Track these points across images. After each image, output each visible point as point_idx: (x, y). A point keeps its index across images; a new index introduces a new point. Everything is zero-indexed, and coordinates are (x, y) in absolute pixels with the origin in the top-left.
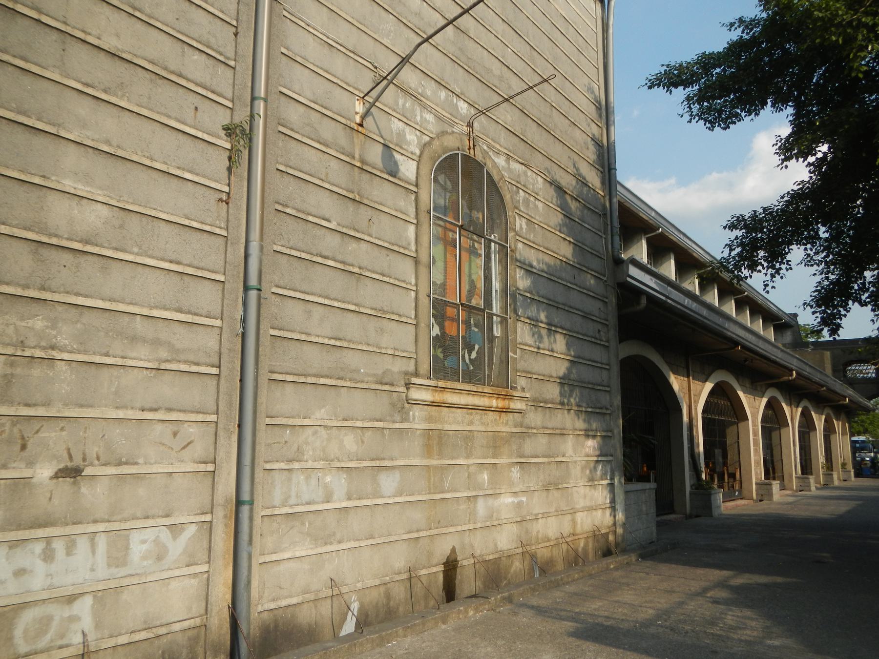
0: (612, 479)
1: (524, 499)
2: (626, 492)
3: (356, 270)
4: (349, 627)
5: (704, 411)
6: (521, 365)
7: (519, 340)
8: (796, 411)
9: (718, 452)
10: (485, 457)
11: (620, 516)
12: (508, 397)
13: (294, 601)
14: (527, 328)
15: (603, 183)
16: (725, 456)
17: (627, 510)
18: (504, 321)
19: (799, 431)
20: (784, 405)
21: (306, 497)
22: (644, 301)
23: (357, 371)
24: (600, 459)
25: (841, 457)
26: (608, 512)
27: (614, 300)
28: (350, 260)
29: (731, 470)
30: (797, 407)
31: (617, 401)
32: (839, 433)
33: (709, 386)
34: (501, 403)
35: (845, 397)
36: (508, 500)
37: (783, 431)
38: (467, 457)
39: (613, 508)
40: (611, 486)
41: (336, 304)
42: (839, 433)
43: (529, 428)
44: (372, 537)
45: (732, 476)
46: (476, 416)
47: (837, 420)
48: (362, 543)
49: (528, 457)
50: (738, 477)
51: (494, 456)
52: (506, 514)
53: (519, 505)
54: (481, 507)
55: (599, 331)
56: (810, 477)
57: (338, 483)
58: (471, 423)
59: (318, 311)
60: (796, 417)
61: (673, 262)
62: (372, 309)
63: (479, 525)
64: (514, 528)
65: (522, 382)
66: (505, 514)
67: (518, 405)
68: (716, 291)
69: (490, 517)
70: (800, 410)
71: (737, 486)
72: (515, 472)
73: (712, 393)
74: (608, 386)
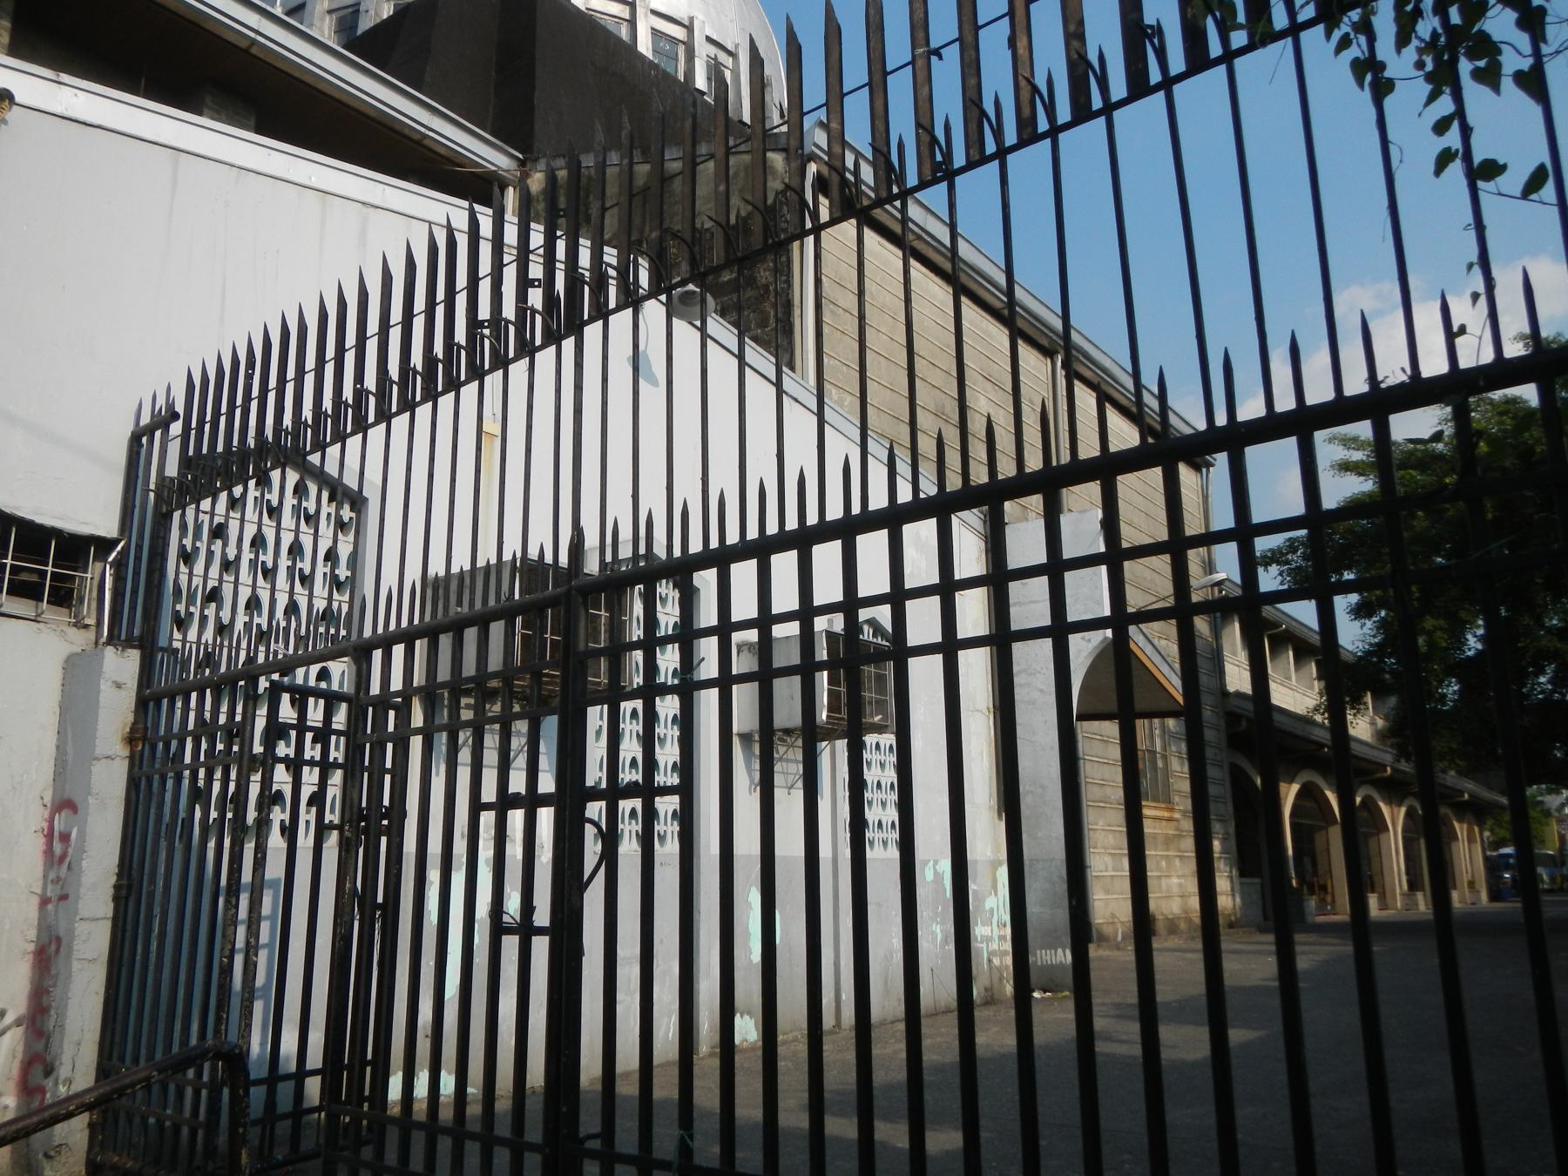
0: (1231, 872)
1: (1183, 881)
2: (1241, 884)
3: (1105, 739)
4: (1119, 938)
5: (1292, 815)
6: (1176, 787)
7: (1173, 769)
8: (1399, 812)
9: (1307, 860)
10: (1163, 851)
11: (1238, 900)
12: (1172, 810)
13: (1101, 921)
14: (1176, 759)
15: (1211, 630)
16: (1314, 864)
17: (1242, 898)
18: (1165, 757)
19: (1404, 838)
20: (1382, 804)
21: (1100, 868)
22: (1244, 724)
23: (1109, 798)
24: (1223, 855)
25: (1467, 873)
26: (1230, 898)
27: (1223, 723)
28: (1103, 734)
29: (1322, 882)
30: (1400, 805)
31: (1230, 808)
32: (1463, 840)
33: (1295, 788)
34: (1166, 814)
35: (1462, 793)
36: (1175, 880)
37: (1383, 837)
38: (1155, 851)
39: (1233, 896)
40: (1231, 878)
41: (1101, 760)
42: (1463, 840)
43: (1182, 831)
44: (1122, 894)
45: (1324, 888)
46: (1157, 824)
47: (1460, 821)
48: (1120, 896)
49: (1183, 852)
50: (1330, 890)
51: (1167, 850)
52: (1175, 890)
53: (1180, 885)
54: (1164, 881)
55: (1216, 754)
56: (1418, 893)
57: (1108, 859)
58: (1155, 828)
59: (1096, 765)
60: (1398, 819)
61: (1237, 625)
62: (1113, 760)
63: (1164, 895)
64: (1178, 900)
65: (1177, 799)
66: (1175, 890)
67: (1177, 816)
68: (1291, 653)
69: (1168, 891)
70: (1403, 810)
71: (1329, 899)
72: (1177, 860)
73: (1299, 795)
74: (1224, 798)
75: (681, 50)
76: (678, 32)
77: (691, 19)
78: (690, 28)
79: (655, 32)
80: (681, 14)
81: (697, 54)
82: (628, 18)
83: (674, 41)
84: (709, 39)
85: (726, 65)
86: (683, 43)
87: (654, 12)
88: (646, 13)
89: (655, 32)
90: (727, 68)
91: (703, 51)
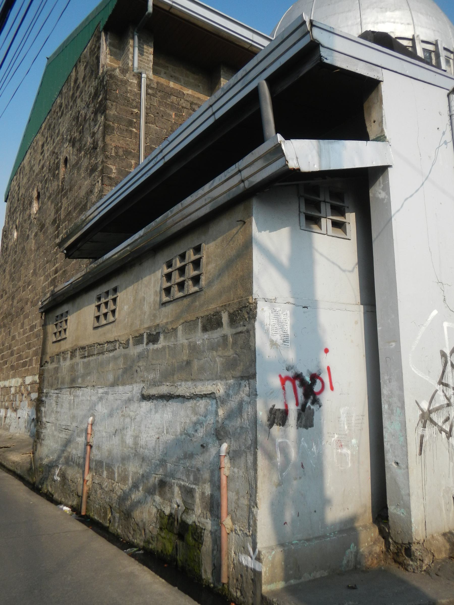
75: (433, 55)
76: (431, 47)
77: (437, 41)
78: (436, 45)
79: (424, 50)
80: (432, 40)
81: (441, 55)
82: (411, 45)
83: (430, 52)
84: (445, 49)
85: (450, 57)
86: (433, 51)
87: (423, 42)
88: (419, 42)
89: (424, 50)
90: (450, 59)
91: (443, 54)
